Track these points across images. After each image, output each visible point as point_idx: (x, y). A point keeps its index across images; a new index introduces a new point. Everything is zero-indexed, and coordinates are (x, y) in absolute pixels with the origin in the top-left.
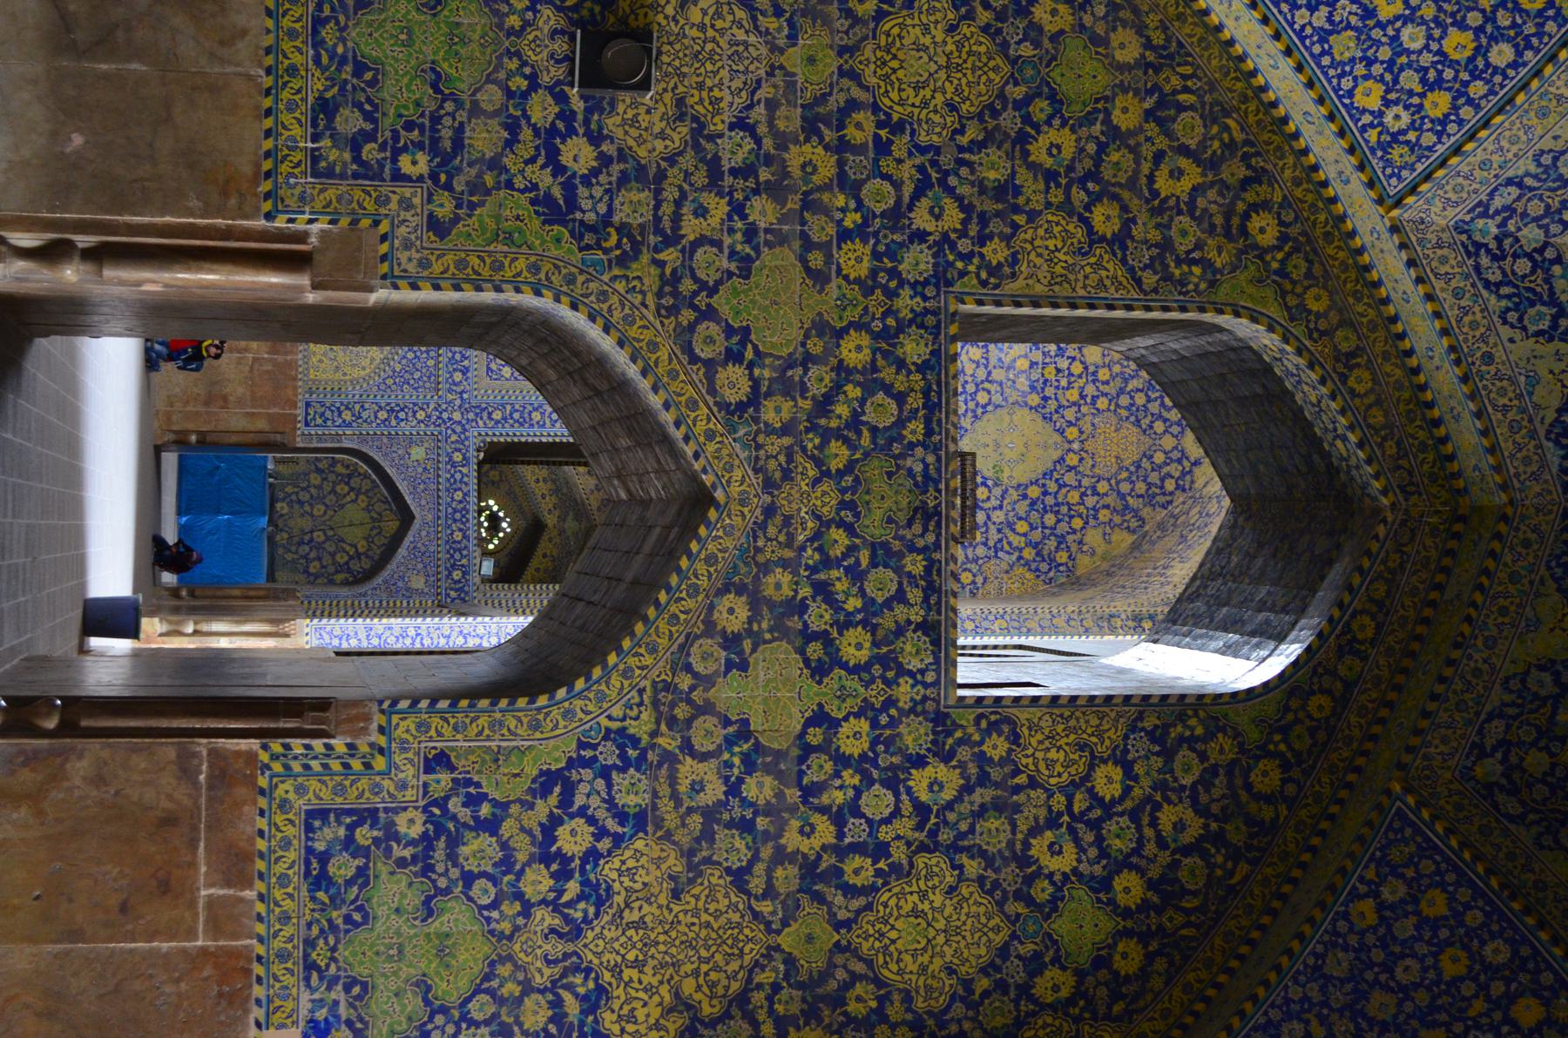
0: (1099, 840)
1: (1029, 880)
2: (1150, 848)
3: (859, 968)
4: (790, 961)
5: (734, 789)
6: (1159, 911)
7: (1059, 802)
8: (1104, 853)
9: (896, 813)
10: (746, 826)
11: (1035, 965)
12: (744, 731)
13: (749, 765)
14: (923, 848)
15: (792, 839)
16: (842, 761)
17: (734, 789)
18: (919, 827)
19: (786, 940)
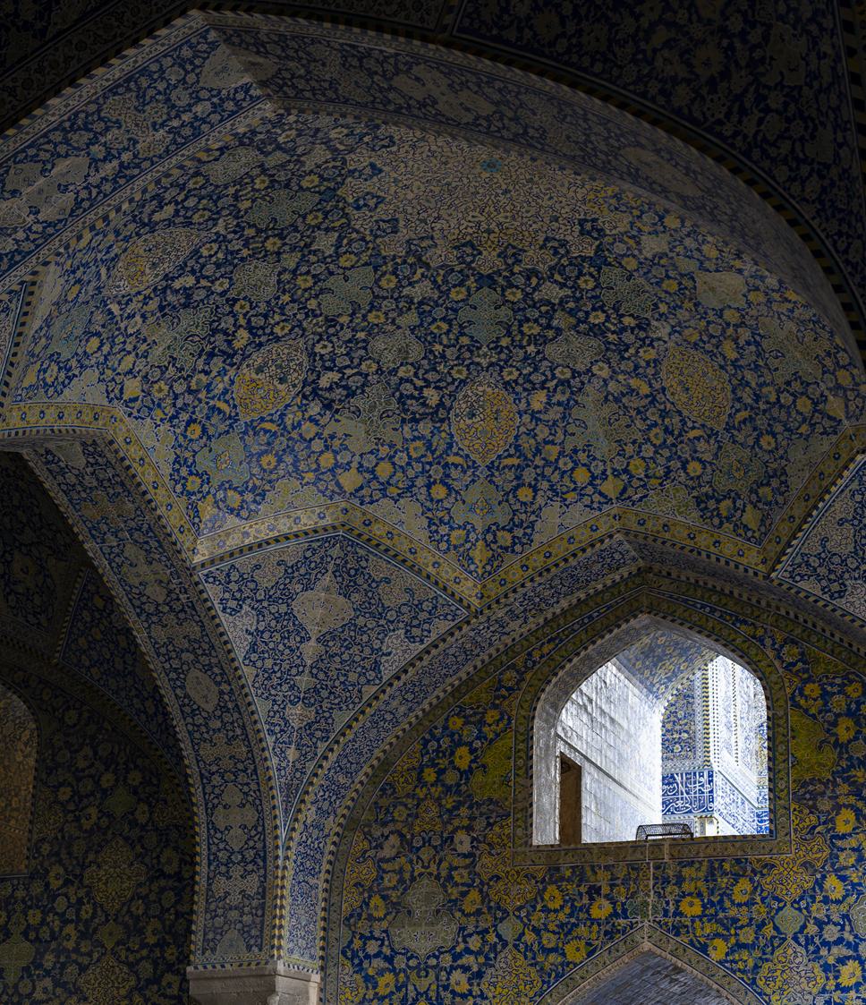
0: (87, 796)
1: (99, 828)
2: (93, 771)
3: (125, 909)
4: (118, 944)
5: (48, 973)
6: (118, 764)
7: (70, 817)
8: (92, 794)
9: (66, 895)
10: (63, 966)
11: (134, 824)
12: (26, 969)
13: (39, 966)
14: (81, 881)
15: (70, 945)
16: (43, 922)
17: (48, 973)
18: (72, 883)
19: (109, 945)
